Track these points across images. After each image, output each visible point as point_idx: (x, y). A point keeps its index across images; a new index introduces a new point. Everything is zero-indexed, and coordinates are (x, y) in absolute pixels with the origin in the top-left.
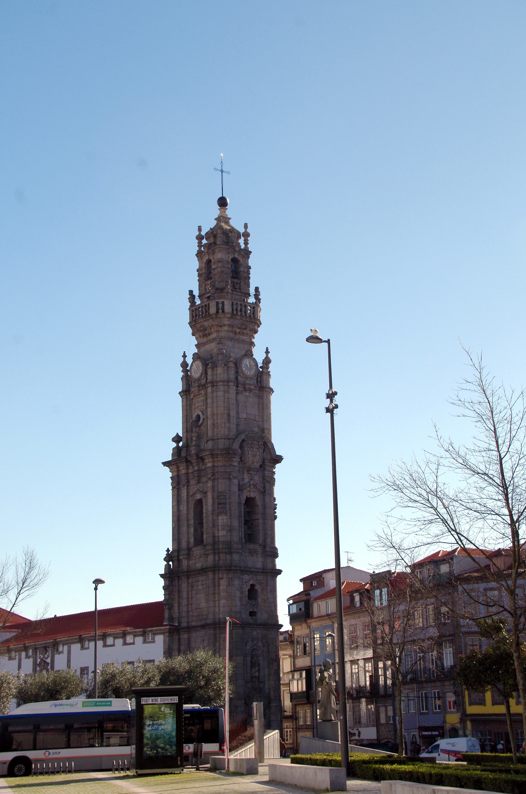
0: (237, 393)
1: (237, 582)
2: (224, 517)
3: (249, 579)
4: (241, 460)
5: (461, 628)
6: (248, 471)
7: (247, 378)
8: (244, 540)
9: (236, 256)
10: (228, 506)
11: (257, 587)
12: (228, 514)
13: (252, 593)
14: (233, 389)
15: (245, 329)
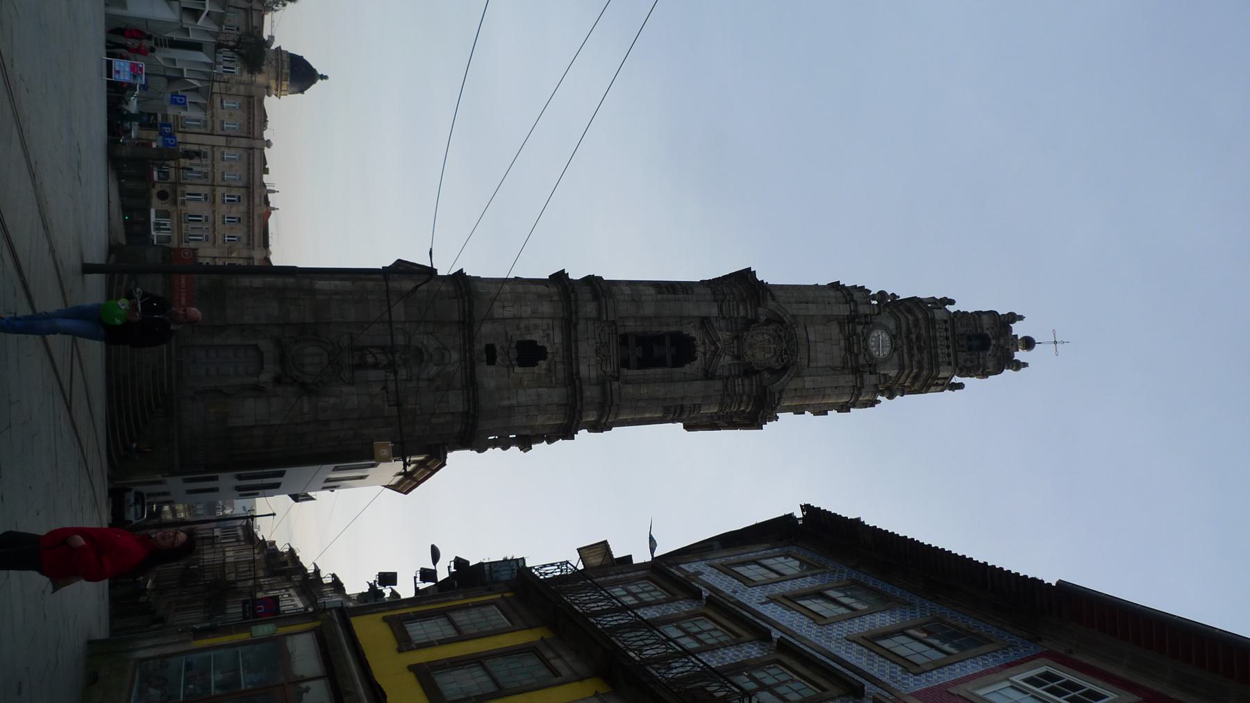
0: (842, 322)
1: (546, 308)
2: (652, 291)
3: (553, 341)
4: (749, 323)
5: (670, 566)
6: (737, 337)
7: (865, 339)
8: (621, 331)
9: (993, 342)
10: (671, 296)
11: (543, 364)
12: (659, 297)
13: (529, 353)
14: (844, 310)
15: (920, 349)
